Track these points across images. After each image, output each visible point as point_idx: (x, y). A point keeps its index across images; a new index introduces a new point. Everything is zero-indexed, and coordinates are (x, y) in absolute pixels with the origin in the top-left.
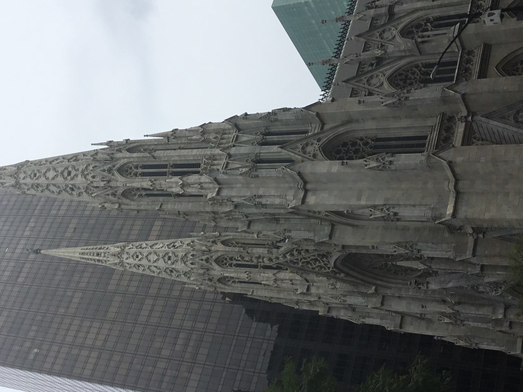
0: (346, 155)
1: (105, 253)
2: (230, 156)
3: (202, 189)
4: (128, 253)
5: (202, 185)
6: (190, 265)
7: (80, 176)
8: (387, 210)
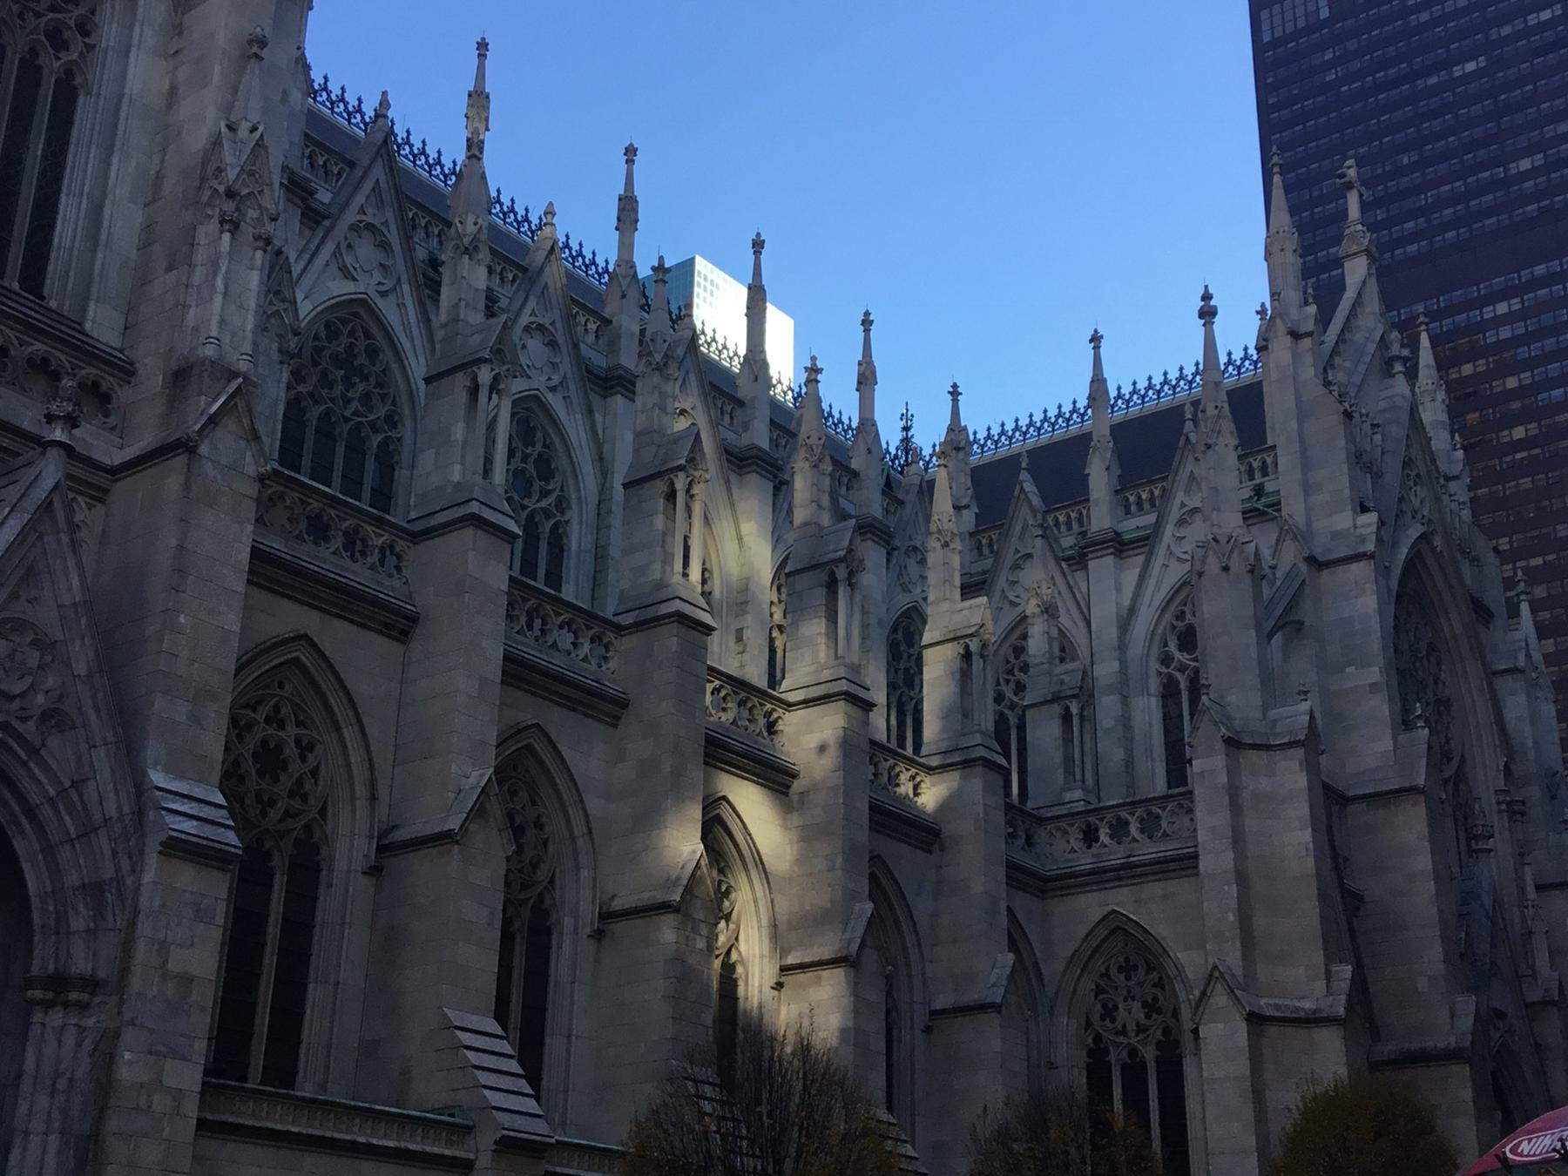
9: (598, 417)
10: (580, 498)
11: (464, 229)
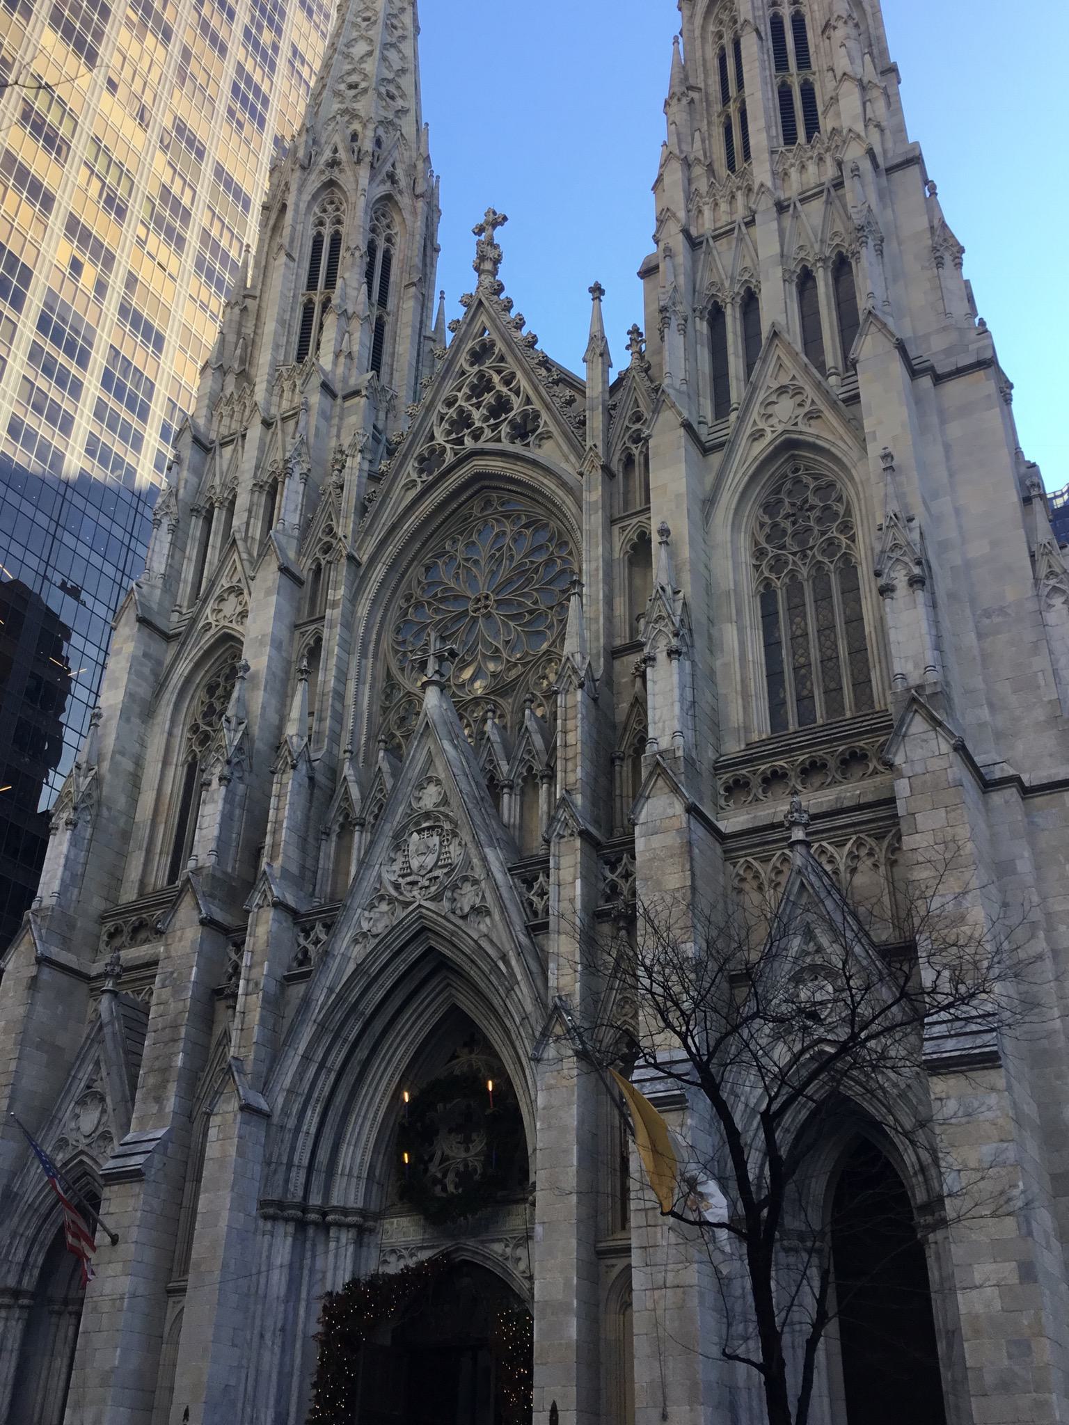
4: (403, 10)
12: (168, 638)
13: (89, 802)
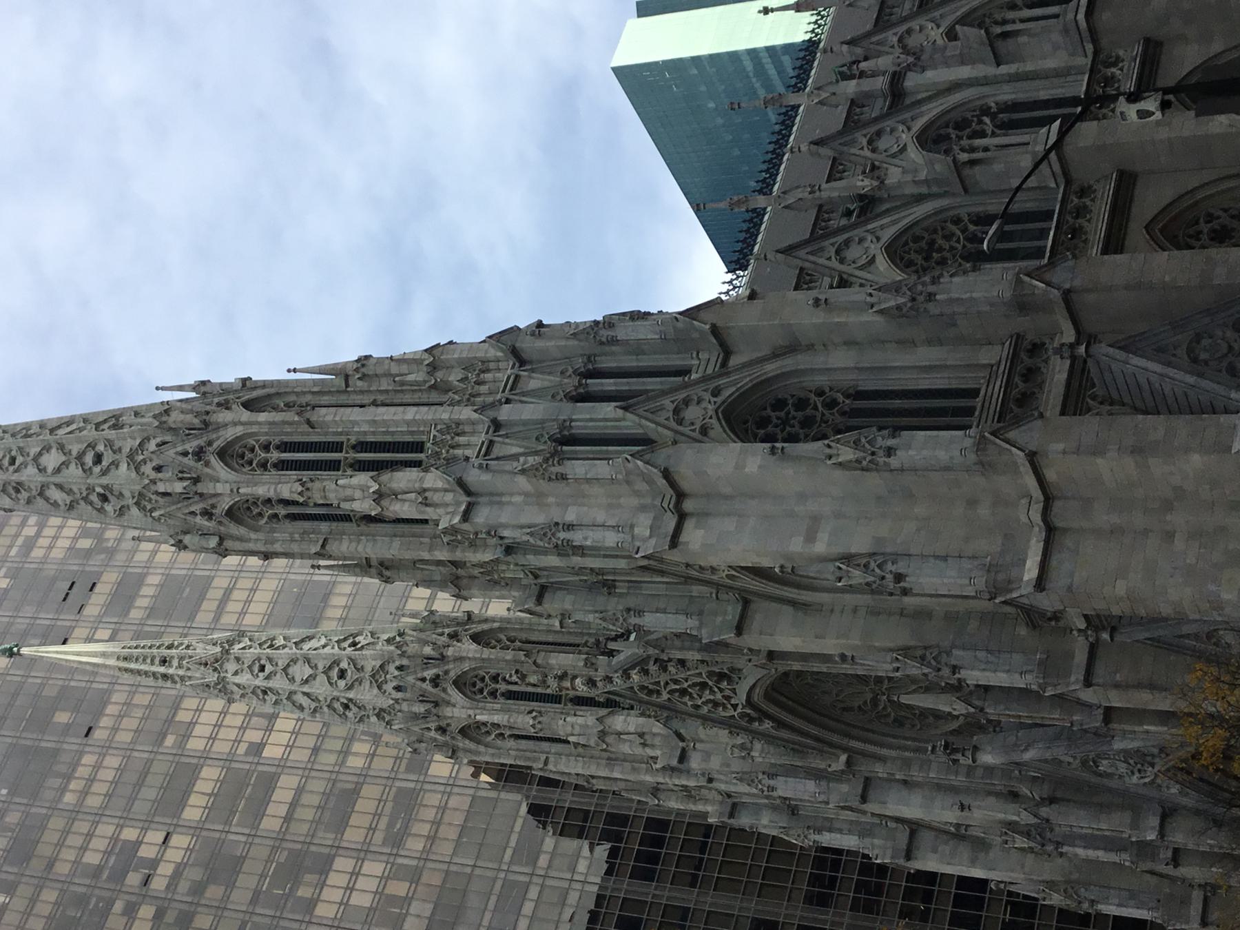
0: (782, 431)
1: (181, 658)
2: (497, 425)
3: (427, 505)
4: (238, 659)
5: (427, 494)
6: (394, 692)
7: (124, 467)
8: (879, 566)
9: (919, 97)
10: (978, 99)
11: (867, 186)
12: (913, 834)
13: (1070, 890)
